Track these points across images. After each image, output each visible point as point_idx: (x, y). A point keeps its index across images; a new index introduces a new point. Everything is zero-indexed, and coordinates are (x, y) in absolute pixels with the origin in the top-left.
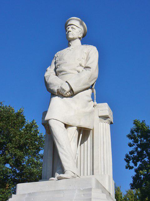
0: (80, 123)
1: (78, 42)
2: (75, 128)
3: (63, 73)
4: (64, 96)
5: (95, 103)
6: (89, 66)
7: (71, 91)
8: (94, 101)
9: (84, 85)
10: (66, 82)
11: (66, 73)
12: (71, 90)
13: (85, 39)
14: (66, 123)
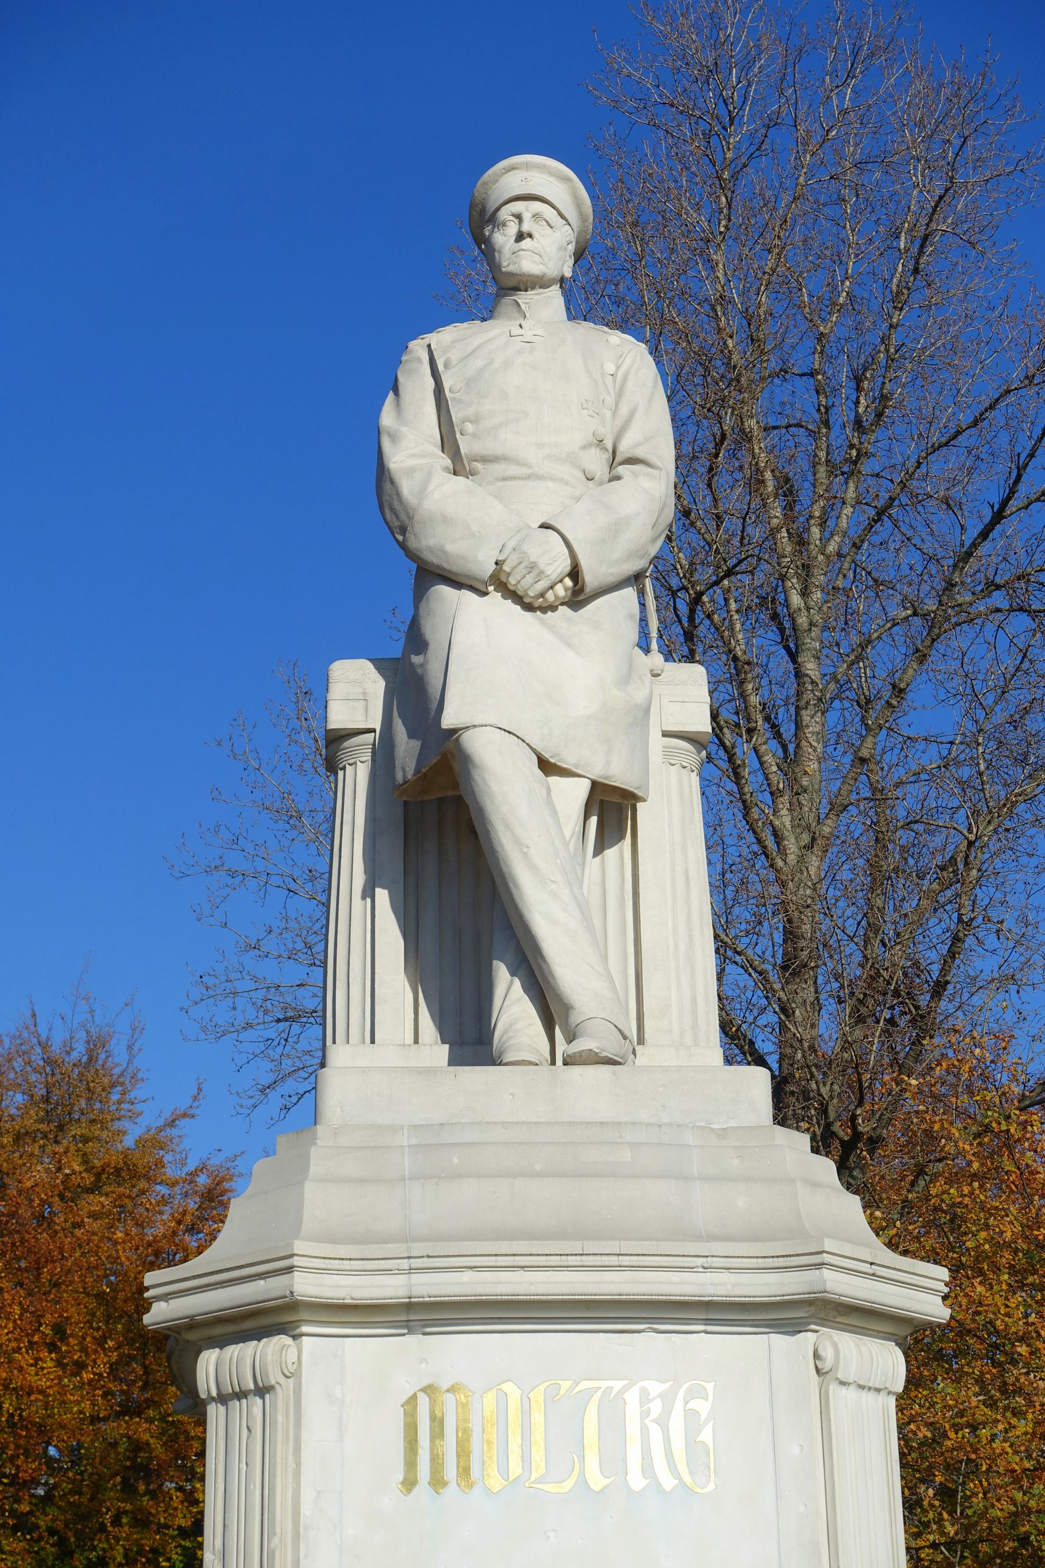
0: (608, 763)
1: (553, 300)
2: (577, 791)
3: (513, 470)
4: (527, 600)
5: (656, 658)
6: (639, 453)
7: (568, 582)
8: (647, 651)
9: (630, 555)
10: (544, 526)
11: (525, 471)
12: (575, 573)
13: (597, 291)
14: (547, 756)
